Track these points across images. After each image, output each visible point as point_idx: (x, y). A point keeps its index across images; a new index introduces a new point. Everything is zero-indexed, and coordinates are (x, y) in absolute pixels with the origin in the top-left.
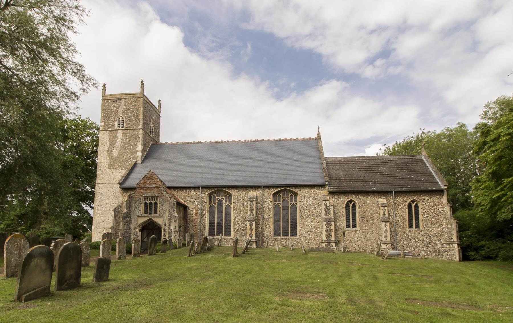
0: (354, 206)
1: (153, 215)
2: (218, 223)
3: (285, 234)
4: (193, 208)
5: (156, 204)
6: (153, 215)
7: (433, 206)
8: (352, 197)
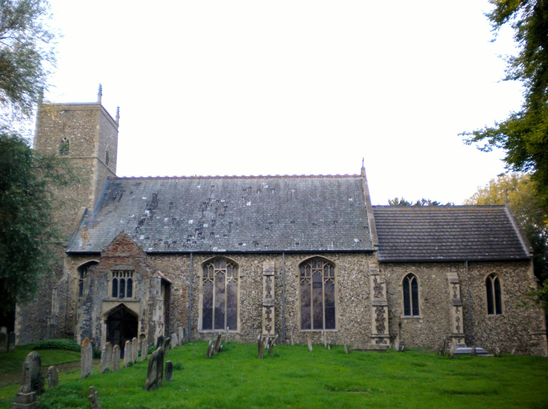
0: (415, 282)
1: (126, 298)
2: (216, 309)
3: (318, 325)
4: (178, 285)
5: (130, 282)
6: (126, 298)
7: (518, 282)
8: (412, 270)
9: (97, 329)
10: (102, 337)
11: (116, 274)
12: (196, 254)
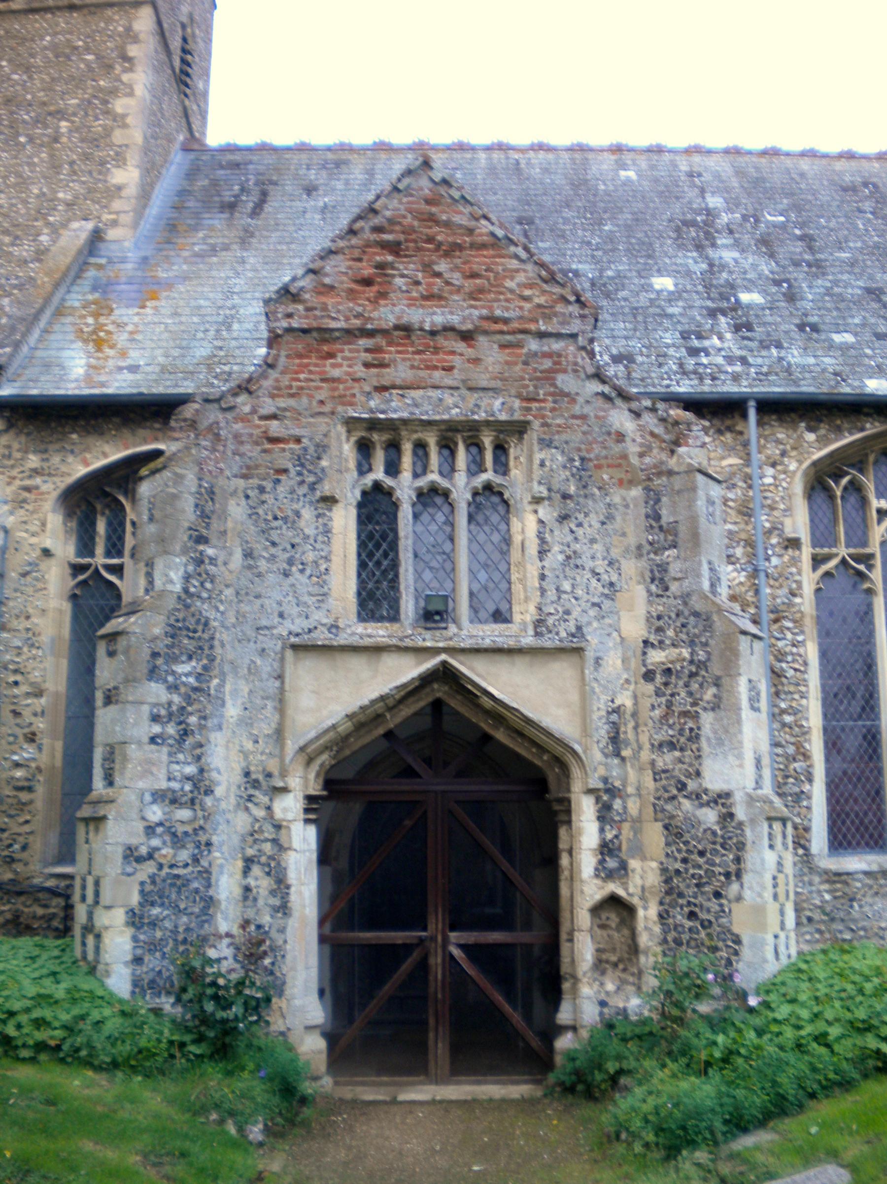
9: (249, 862)
10: (292, 923)
11: (379, 458)
12: (781, 409)
